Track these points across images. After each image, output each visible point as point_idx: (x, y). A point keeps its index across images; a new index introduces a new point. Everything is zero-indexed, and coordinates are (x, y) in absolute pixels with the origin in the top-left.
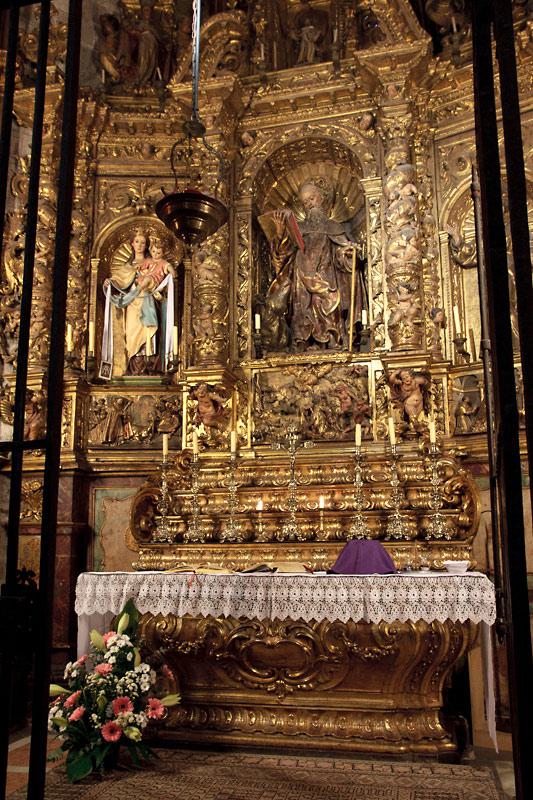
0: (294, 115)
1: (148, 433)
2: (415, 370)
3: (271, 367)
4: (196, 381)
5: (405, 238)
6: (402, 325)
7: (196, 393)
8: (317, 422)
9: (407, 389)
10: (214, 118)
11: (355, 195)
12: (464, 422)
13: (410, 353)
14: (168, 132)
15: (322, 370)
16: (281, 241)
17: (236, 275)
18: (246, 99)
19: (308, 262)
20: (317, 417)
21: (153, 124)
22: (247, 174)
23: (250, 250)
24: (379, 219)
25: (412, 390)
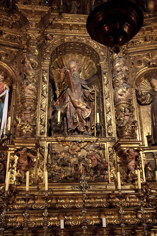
0: (70, 32)
3: (57, 141)
4: (21, 146)
5: (125, 88)
6: (127, 127)
7: (19, 152)
8: (81, 171)
9: (130, 158)
10: (36, 24)
11: (91, 69)
13: (131, 140)
14: (10, 27)
15: (83, 145)
16: (62, 83)
17: (40, 95)
18: (51, 20)
19: (74, 94)
20: (81, 167)
21: (4, 21)
22: (48, 51)
24: (108, 80)
25: (133, 158)
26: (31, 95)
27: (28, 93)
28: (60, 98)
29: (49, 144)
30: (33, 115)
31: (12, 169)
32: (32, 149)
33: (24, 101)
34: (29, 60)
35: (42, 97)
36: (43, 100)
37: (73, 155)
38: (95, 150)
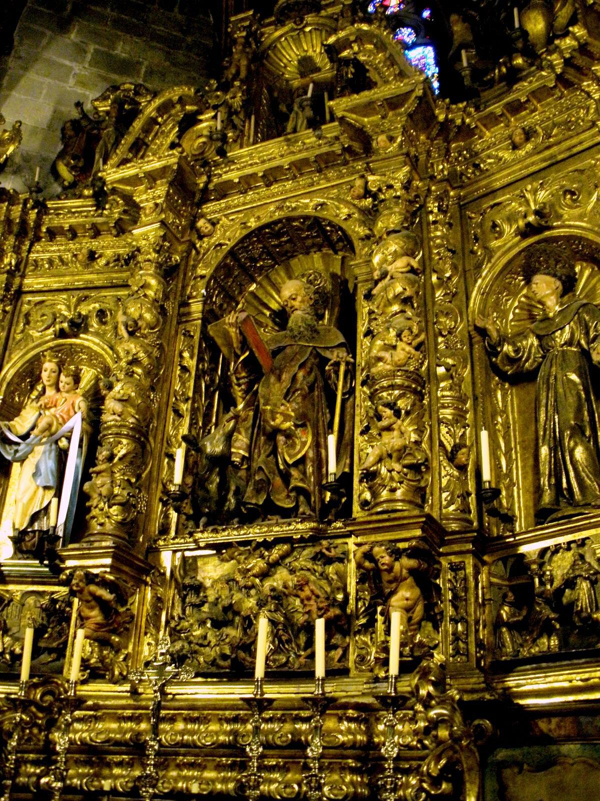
0: (268, 193)
2: (401, 545)
3: (199, 548)
10: (157, 205)
12: (507, 637)
14: (114, 232)
37: (246, 587)
38: (316, 567)
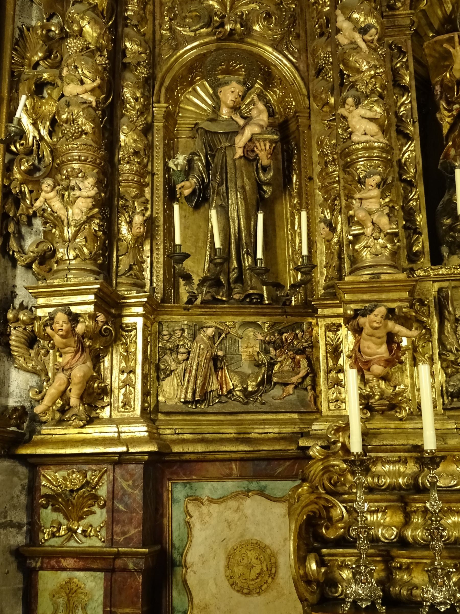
1: (258, 385)
7: (361, 320)
23: (413, 93)
26: (372, 136)
27: (362, 131)
28: (456, 133)
29: (440, 290)
30: (387, 200)
31: (337, 373)
32: (400, 308)
33: (352, 160)
34: (349, 19)
35: (399, 140)
36: (405, 149)
